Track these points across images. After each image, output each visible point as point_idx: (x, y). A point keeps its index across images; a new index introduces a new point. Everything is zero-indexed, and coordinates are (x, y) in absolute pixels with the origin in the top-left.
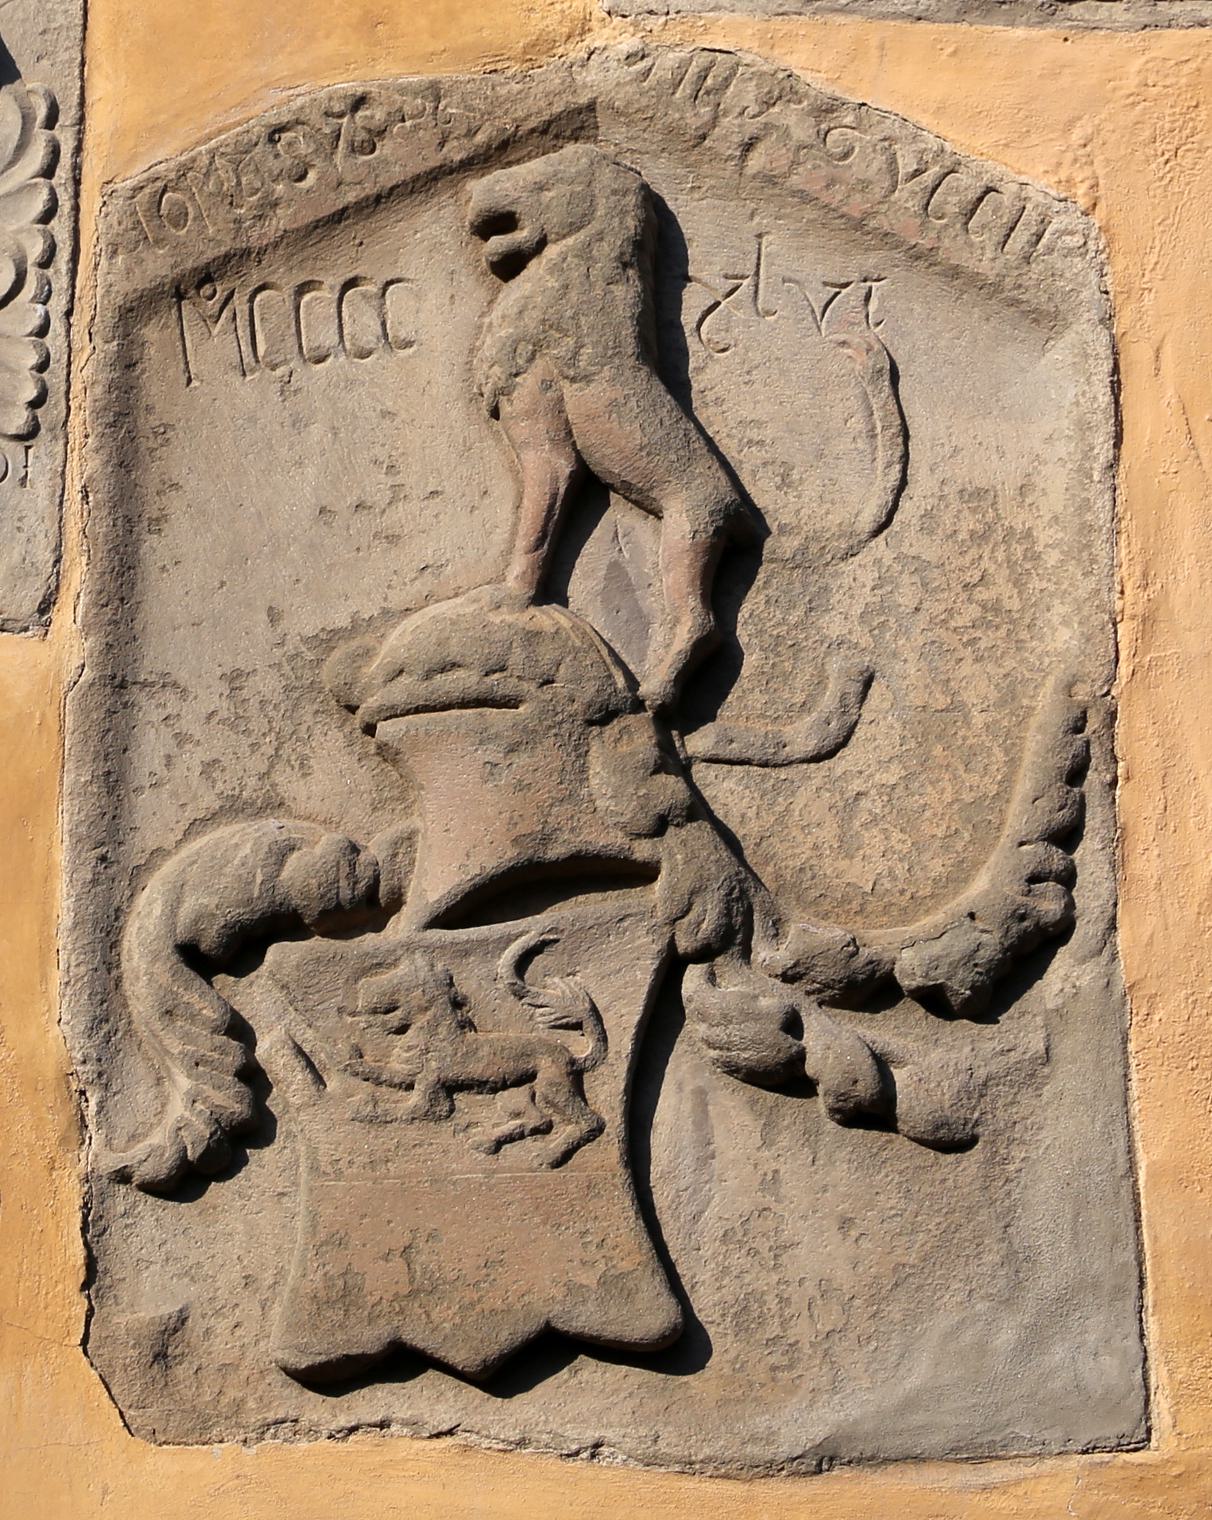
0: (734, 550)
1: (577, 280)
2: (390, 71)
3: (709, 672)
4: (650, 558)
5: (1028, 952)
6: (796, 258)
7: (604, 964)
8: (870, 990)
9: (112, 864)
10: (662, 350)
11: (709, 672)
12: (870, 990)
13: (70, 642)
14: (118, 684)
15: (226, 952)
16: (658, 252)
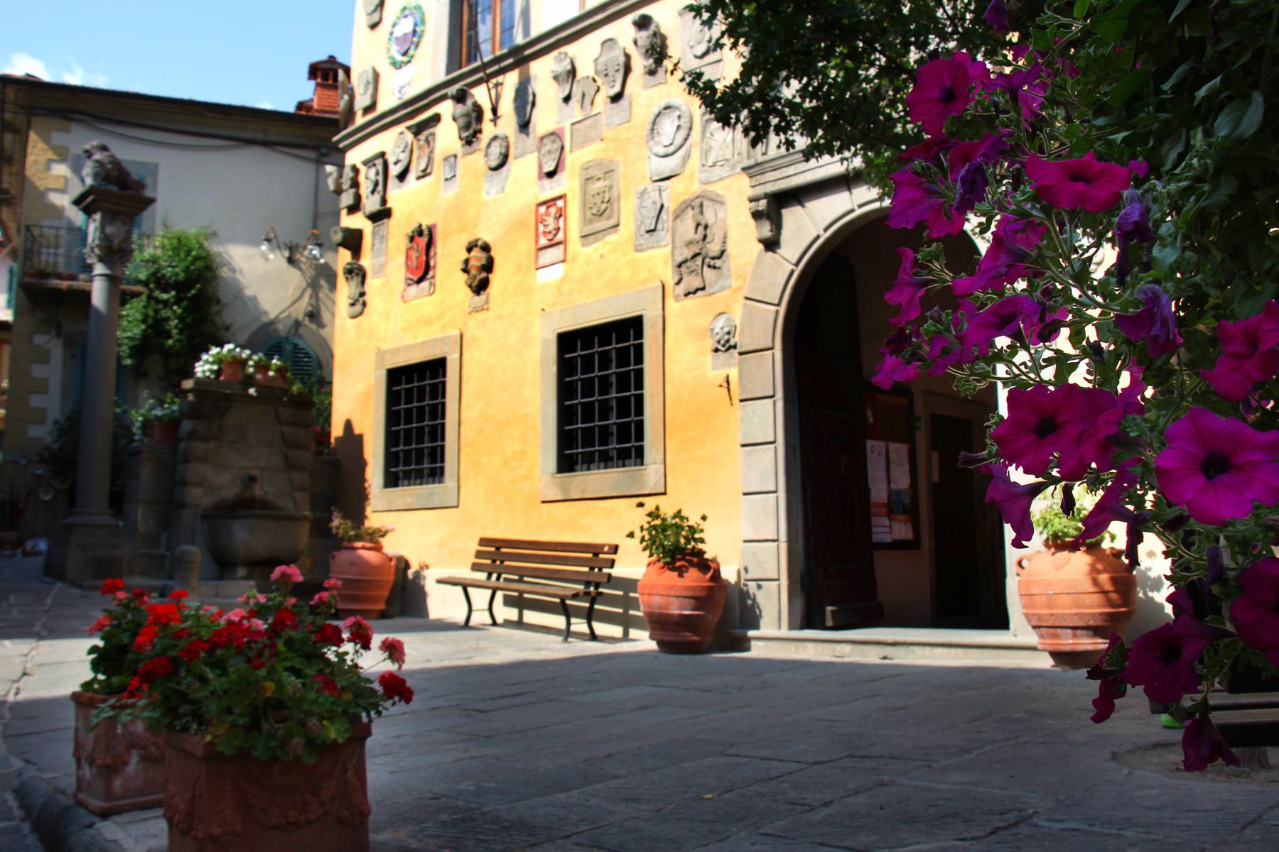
0: (706, 227)
1: (697, 210)
2: (685, 197)
3: (705, 237)
4: (700, 229)
5: (723, 252)
6: (710, 203)
7: (699, 261)
8: (713, 258)
9: (673, 260)
10: (702, 213)
11: (705, 237)
12: (713, 258)
13: (669, 248)
14: (673, 248)
15: (679, 266)
16: (701, 205)
